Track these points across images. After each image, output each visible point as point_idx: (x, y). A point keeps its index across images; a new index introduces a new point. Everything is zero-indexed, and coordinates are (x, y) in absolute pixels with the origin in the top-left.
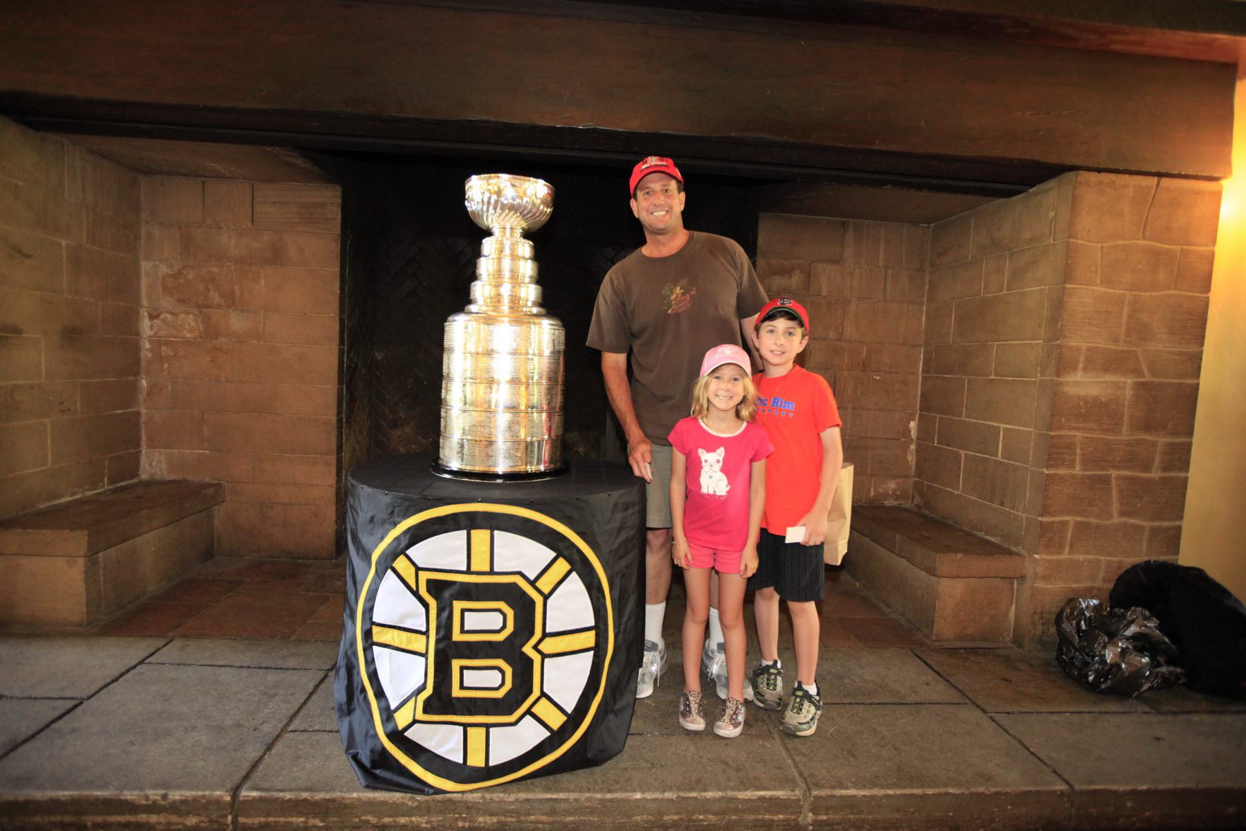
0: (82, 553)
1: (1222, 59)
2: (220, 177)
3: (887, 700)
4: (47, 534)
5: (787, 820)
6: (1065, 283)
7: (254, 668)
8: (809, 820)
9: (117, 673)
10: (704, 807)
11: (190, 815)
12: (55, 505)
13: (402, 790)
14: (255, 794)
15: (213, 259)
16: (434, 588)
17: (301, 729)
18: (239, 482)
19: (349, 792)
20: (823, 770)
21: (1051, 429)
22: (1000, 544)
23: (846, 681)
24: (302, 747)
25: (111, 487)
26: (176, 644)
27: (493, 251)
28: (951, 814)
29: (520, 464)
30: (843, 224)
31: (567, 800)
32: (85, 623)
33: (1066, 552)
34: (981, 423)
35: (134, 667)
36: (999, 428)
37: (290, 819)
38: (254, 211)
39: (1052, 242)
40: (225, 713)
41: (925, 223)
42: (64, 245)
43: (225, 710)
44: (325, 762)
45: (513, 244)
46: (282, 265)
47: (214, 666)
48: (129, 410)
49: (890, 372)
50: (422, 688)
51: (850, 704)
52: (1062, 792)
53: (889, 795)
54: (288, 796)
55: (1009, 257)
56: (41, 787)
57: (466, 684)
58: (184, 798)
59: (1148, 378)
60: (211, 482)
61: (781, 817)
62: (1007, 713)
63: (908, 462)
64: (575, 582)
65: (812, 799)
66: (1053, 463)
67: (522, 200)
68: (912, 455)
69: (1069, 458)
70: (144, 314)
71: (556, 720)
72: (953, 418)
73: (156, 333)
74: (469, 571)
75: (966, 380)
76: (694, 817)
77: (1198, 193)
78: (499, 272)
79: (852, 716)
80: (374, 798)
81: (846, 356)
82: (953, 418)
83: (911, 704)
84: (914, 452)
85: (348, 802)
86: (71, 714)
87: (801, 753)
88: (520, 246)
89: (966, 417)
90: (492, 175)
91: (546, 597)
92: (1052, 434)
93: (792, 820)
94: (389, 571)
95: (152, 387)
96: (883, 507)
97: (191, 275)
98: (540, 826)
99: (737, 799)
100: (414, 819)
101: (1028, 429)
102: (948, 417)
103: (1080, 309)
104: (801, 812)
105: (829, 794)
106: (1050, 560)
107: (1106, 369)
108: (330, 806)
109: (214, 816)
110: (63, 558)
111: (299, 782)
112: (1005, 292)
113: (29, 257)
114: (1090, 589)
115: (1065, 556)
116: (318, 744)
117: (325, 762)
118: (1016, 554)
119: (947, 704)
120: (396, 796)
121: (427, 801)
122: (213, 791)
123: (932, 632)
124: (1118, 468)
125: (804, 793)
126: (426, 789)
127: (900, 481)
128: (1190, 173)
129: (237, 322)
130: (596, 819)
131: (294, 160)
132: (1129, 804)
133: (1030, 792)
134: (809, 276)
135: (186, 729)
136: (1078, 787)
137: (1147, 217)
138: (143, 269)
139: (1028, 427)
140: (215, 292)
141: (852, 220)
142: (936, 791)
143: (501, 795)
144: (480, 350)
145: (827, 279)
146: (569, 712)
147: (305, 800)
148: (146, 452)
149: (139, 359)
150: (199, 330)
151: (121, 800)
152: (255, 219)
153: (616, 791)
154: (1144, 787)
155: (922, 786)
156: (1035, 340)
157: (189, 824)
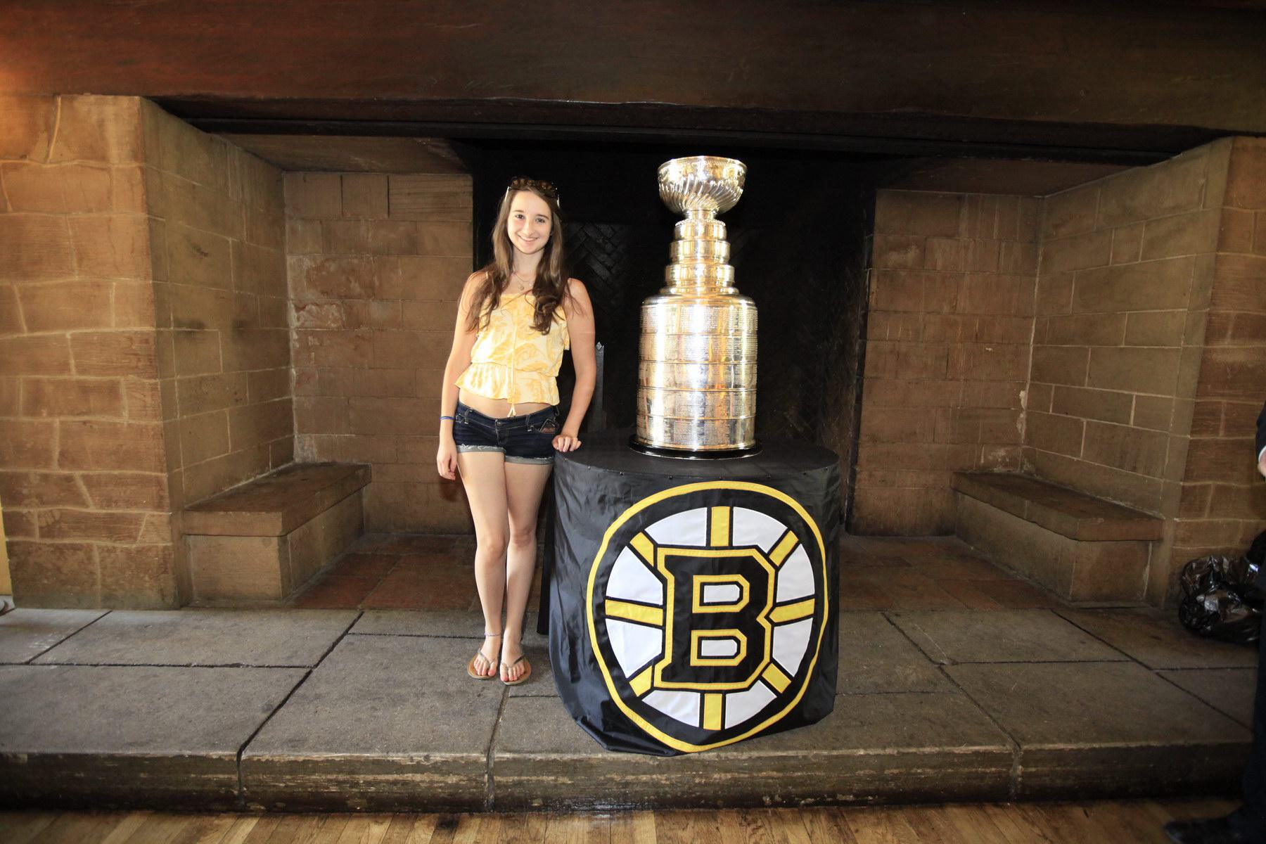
2: (358, 170)
3: (1052, 659)
4: (246, 516)
5: (1000, 772)
6: (1218, 251)
7: (450, 637)
9: (330, 644)
10: (923, 760)
11: (451, 775)
12: (238, 489)
14: (508, 755)
15: (353, 251)
16: (671, 562)
17: (520, 695)
18: (384, 464)
19: (595, 753)
20: (1024, 726)
22: (1132, 508)
24: (528, 711)
25: (275, 470)
26: (369, 615)
27: (689, 234)
29: (727, 440)
30: (959, 198)
31: (797, 756)
32: (281, 596)
33: (1206, 515)
35: (341, 638)
36: (1132, 396)
37: (540, 778)
38: (391, 202)
39: (1202, 206)
40: (444, 680)
41: (1040, 194)
42: (230, 242)
43: (443, 677)
45: (707, 227)
46: (417, 254)
47: (411, 636)
48: (284, 398)
50: (661, 657)
51: (1019, 662)
53: (1095, 748)
54: (539, 757)
55: (1146, 226)
56: (315, 749)
57: (703, 654)
58: (444, 759)
60: (360, 464)
61: (993, 769)
63: (1018, 431)
64: (801, 555)
65: (1022, 753)
66: (1197, 429)
68: (1022, 423)
70: (291, 306)
71: (782, 684)
72: (1073, 387)
73: (303, 324)
75: (1090, 349)
76: (913, 771)
78: (692, 258)
80: (620, 759)
81: (960, 328)
83: (1075, 662)
85: (594, 762)
86: (307, 680)
87: (994, 710)
88: (715, 228)
89: (1089, 385)
90: (690, 158)
91: (777, 569)
92: (1198, 401)
93: (1005, 772)
94: (626, 549)
95: (301, 375)
97: (333, 267)
98: (770, 781)
99: (953, 753)
100: (654, 776)
102: (1068, 386)
104: (1011, 765)
107: (1255, 335)
109: (473, 776)
110: (260, 538)
112: (1140, 261)
113: (206, 255)
115: (1204, 519)
116: (543, 708)
119: (1109, 661)
121: (667, 760)
122: (469, 753)
123: (1069, 594)
125: (1014, 749)
126: (666, 751)
127: (1009, 448)
129: (377, 311)
130: (823, 774)
131: (439, 151)
134: (925, 250)
135: (416, 695)
138: (288, 263)
139: (1170, 395)
141: (967, 194)
143: (735, 754)
145: (943, 253)
146: (793, 676)
147: (555, 761)
148: (298, 438)
149: (288, 351)
150: (342, 319)
151: (389, 761)
152: (391, 210)
153: (840, 748)
155: (1124, 740)
156: (1179, 308)
157: (450, 782)
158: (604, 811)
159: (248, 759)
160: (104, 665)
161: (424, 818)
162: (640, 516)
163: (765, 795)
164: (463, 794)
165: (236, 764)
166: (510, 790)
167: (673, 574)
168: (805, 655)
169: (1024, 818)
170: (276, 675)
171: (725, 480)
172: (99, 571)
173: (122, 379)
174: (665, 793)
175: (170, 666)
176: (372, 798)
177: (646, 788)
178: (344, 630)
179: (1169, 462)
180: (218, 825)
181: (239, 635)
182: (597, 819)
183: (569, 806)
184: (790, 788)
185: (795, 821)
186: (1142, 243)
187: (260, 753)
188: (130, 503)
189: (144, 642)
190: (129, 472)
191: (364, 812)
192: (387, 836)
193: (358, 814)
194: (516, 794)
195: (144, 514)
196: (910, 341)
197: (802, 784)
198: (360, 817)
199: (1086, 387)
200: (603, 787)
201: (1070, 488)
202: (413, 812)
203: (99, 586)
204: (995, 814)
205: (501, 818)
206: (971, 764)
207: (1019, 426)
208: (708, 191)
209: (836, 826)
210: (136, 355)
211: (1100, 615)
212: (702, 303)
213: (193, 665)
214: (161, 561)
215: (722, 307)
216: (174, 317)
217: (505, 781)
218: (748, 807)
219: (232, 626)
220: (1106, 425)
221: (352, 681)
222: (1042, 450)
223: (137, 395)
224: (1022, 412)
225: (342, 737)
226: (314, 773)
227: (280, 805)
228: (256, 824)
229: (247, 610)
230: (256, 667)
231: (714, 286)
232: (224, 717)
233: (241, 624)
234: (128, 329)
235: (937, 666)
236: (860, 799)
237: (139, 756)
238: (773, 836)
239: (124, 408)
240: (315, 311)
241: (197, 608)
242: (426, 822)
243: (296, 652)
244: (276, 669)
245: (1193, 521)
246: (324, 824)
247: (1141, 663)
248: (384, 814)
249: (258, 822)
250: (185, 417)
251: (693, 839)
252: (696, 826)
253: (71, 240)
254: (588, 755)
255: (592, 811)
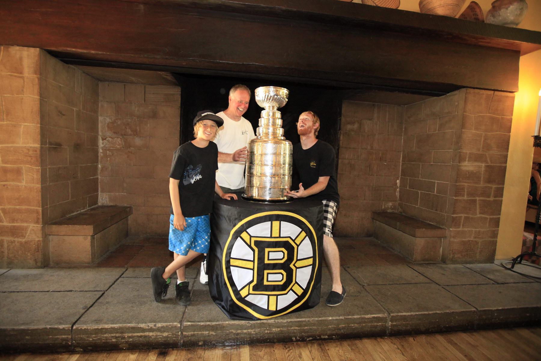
0: (91, 234)
1: (515, 49)
2: (132, 82)
3: (405, 283)
4: (77, 227)
6: (462, 129)
8: (390, 325)
9: (113, 281)
10: (354, 321)
11: (165, 332)
12: (73, 216)
13: (244, 319)
14: (189, 323)
19: (225, 321)
20: (392, 307)
21: (456, 181)
23: (388, 276)
25: (89, 208)
28: (437, 320)
30: (374, 105)
31: (306, 321)
33: (461, 227)
34: (427, 181)
36: (435, 182)
41: (404, 105)
42: (75, 110)
44: (210, 311)
45: (274, 114)
48: (95, 177)
49: (390, 161)
50: (252, 281)
51: (392, 284)
52: (474, 311)
53: (417, 315)
54: (202, 324)
55: (439, 119)
56: (106, 323)
57: (269, 280)
59: (490, 164)
60: (127, 206)
61: (380, 324)
62: (447, 285)
63: (396, 195)
64: (307, 241)
65: (391, 317)
67: (280, 96)
68: (398, 193)
69: (463, 193)
70: (100, 138)
71: (300, 292)
72: (415, 179)
73: (105, 146)
74: (271, 237)
76: (350, 325)
77: (507, 97)
78: (268, 125)
79: (395, 288)
80: (234, 323)
82: (415, 179)
83: (413, 284)
84: (399, 192)
85: (225, 325)
88: (277, 114)
89: (421, 178)
91: (298, 246)
92: (457, 184)
93: (385, 325)
94: (239, 238)
95: (102, 168)
96: (387, 212)
98: (295, 331)
99: (365, 318)
100: (249, 330)
101: (447, 183)
103: (467, 138)
104: (387, 322)
105: (397, 315)
106: (456, 231)
107: (476, 161)
108: (218, 327)
109: (174, 332)
111: (204, 318)
112: (437, 132)
113: (64, 115)
114: (469, 241)
115: (460, 229)
117: (210, 311)
118: (443, 229)
119: (426, 283)
120: (243, 322)
121: (254, 323)
122: (173, 323)
123: (413, 258)
124: (479, 197)
125: (388, 316)
127: (393, 202)
128: (505, 90)
129: (138, 141)
130: (316, 327)
132: (496, 314)
133: (464, 311)
135: (151, 301)
136: (479, 309)
137: (490, 106)
138: (99, 120)
139: (448, 181)
140: (129, 129)
141: (376, 104)
142: (433, 312)
143: (281, 320)
144: (263, 153)
145: (367, 125)
146: (304, 288)
147: (209, 325)
148: (100, 194)
149: (98, 157)
150: (122, 144)
151: (138, 327)
153: (322, 317)
154: (501, 308)
155: (427, 311)
157: (164, 336)
158: (228, 346)
159: (76, 329)
160: (9, 292)
161: (153, 351)
162: (245, 225)
163: (293, 337)
164: (170, 341)
165: (71, 331)
166: (189, 338)
167: (257, 248)
168: (309, 280)
169: (392, 343)
170: (89, 294)
171: (278, 211)
172: (6, 251)
173: (23, 167)
174: (254, 337)
175: (40, 292)
176: (130, 343)
177: (245, 336)
178: (119, 276)
179: (448, 207)
180: (61, 358)
181: (72, 278)
182: (225, 349)
183: (214, 344)
184: (303, 333)
185: (305, 347)
186: (438, 124)
187: (82, 326)
188: (23, 221)
189: (27, 282)
190: (24, 207)
191: (128, 350)
192: (137, 359)
193: (124, 351)
194: (192, 340)
195: (30, 226)
196: (355, 160)
197: (308, 332)
198: (126, 352)
199: (420, 179)
200: (229, 335)
201: (414, 218)
202: (148, 349)
203: (6, 258)
204: (381, 341)
205: (186, 350)
206: (372, 322)
207: (397, 194)
208: (274, 99)
209: (320, 348)
210: (31, 156)
211: (424, 266)
212: (271, 142)
213: (51, 291)
214: (36, 247)
215: (279, 144)
216: (48, 141)
217: (188, 334)
218: (286, 342)
219: (69, 275)
220: (427, 193)
221: (123, 296)
222: (405, 203)
223: (30, 174)
224: (398, 188)
225: (119, 318)
226: (105, 333)
227: (90, 348)
228: (78, 357)
229: (75, 268)
230: (80, 291)
231: (276, 136)
232: (65, 312)
233: (73, 274)
234: (27, 145)
235: (362, 286)
236: (330, 337)
237: (26, 329)
238: (296, 353)
239: (23, 179)
240: (111, 141)
241: (52, 268)
242: (154, 353)
243: (98, 285)
244: (88, 292)
245: (457, 230)
246: (109, 355)
247: (436, 283)
248: (135, 350)
249: (80, 355)
250: (51, 184)
251: (264, 355)
252: (266, 350)
253: (3, 107)
254: (223, 323)
255: (224, 346)
